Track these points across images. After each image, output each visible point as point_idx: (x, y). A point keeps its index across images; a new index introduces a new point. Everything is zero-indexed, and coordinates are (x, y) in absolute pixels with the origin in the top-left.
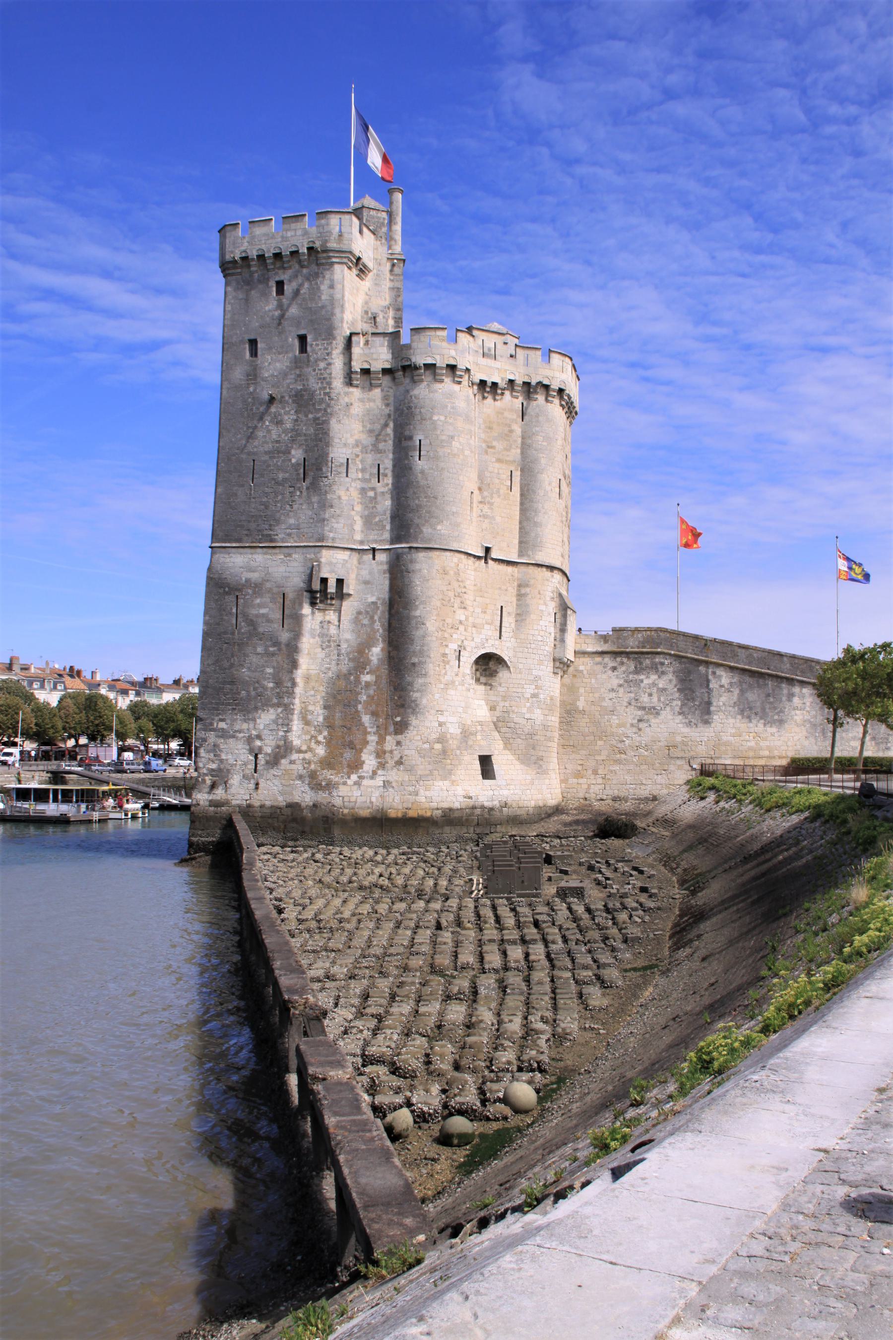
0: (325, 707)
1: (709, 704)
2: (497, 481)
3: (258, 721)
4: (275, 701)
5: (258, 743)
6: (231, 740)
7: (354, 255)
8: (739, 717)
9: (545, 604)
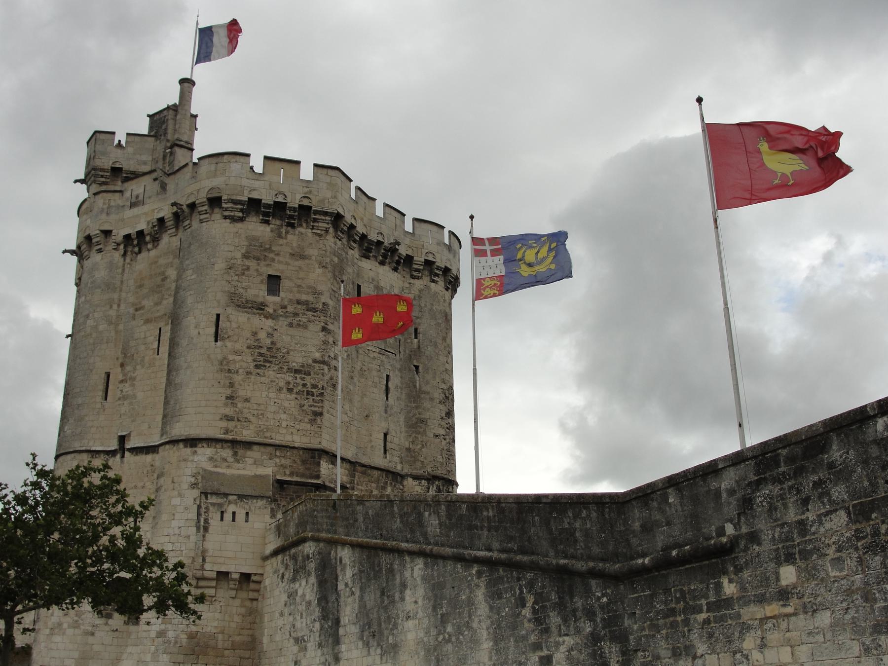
2: (142, 347)
7: (103, 170)
9: (180, 495)
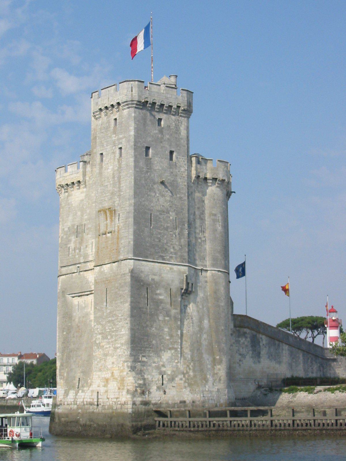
0: (190, 351)
1: (259, 353)
3: (163, 357)
4: (171, 346)
5: (163, 369)
6: (149, 367)
8: (268, 359)
